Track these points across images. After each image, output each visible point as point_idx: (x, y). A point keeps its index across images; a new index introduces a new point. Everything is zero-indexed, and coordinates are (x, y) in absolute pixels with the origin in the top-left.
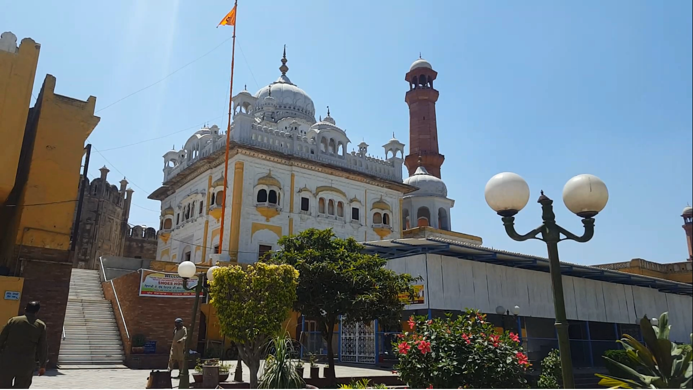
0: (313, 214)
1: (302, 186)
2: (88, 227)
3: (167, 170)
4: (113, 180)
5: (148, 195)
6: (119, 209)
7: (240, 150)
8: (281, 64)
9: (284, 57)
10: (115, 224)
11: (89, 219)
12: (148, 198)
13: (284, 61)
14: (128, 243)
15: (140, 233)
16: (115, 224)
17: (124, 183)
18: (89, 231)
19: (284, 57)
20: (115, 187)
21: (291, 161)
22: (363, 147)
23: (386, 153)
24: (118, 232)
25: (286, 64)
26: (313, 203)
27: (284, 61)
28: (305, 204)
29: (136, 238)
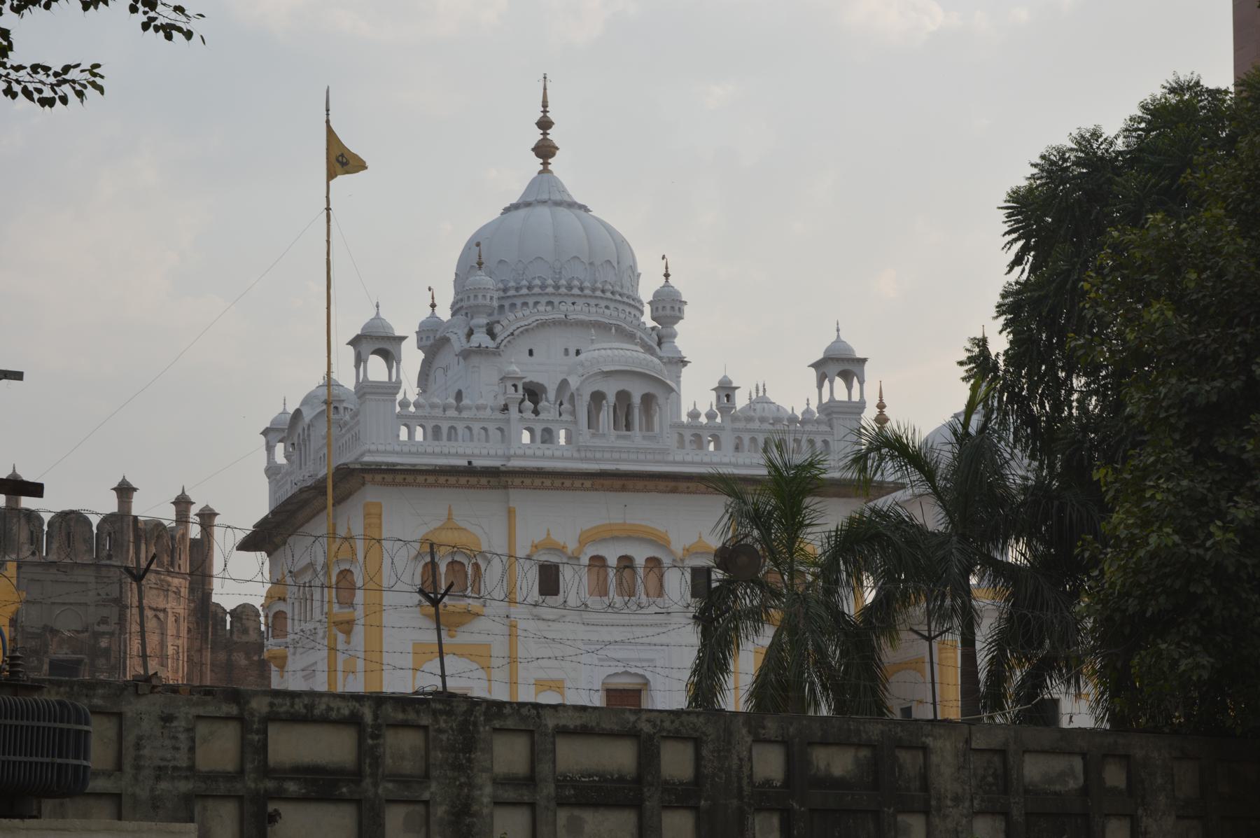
0: (573, 601)
1: (539, 537)
2: (104, 643)
3: (272, 471)
4: (153, 506)
5: (241, 536)
6: (176, 581)
7: (368, 477)
8: (537, 135)
9: (545, 112)
10: (171, 619)
11: (104, 621)
12: (239, 548)
13: (545, 124)
14: (222, 656)
15: (251, 624)
16: (171, 619)
17: (182, 503)
18: (106, 652)
19: (545, 112)
20: (158, 525)
21: (504, 479)
22: (726, 391)
23: (820, 386)
24: (183, 642)
25: (553, 134)
26: (573, 581)
27: (545, 124)
28: (549, 581)
29: (245, 639)
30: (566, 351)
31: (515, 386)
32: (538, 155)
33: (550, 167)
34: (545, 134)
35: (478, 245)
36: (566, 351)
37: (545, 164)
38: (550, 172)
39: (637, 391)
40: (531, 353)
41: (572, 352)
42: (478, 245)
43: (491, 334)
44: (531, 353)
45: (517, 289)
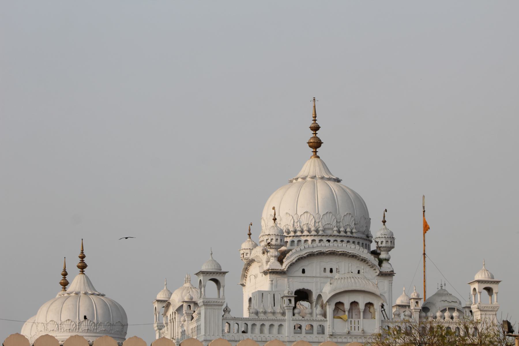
8: (311, 133)
13: (316, 129)
25: (320, 134)
27: (316, 129)
30: (325, 269)
31: (290, 300)
32: (310, 147)
33: (318, 154)
34: (316, 134)
35: (274, 208)
36: (325, 269)
37: (316, 152)
38: (318, 157)
39: (362, 301)
40: (304, 271)
41: (328, 270)
42: (274, 208)
43: (280, 260)
44: (304, 271)
45: (295, 232)
